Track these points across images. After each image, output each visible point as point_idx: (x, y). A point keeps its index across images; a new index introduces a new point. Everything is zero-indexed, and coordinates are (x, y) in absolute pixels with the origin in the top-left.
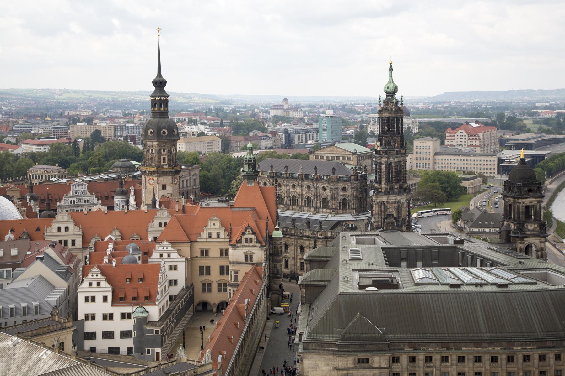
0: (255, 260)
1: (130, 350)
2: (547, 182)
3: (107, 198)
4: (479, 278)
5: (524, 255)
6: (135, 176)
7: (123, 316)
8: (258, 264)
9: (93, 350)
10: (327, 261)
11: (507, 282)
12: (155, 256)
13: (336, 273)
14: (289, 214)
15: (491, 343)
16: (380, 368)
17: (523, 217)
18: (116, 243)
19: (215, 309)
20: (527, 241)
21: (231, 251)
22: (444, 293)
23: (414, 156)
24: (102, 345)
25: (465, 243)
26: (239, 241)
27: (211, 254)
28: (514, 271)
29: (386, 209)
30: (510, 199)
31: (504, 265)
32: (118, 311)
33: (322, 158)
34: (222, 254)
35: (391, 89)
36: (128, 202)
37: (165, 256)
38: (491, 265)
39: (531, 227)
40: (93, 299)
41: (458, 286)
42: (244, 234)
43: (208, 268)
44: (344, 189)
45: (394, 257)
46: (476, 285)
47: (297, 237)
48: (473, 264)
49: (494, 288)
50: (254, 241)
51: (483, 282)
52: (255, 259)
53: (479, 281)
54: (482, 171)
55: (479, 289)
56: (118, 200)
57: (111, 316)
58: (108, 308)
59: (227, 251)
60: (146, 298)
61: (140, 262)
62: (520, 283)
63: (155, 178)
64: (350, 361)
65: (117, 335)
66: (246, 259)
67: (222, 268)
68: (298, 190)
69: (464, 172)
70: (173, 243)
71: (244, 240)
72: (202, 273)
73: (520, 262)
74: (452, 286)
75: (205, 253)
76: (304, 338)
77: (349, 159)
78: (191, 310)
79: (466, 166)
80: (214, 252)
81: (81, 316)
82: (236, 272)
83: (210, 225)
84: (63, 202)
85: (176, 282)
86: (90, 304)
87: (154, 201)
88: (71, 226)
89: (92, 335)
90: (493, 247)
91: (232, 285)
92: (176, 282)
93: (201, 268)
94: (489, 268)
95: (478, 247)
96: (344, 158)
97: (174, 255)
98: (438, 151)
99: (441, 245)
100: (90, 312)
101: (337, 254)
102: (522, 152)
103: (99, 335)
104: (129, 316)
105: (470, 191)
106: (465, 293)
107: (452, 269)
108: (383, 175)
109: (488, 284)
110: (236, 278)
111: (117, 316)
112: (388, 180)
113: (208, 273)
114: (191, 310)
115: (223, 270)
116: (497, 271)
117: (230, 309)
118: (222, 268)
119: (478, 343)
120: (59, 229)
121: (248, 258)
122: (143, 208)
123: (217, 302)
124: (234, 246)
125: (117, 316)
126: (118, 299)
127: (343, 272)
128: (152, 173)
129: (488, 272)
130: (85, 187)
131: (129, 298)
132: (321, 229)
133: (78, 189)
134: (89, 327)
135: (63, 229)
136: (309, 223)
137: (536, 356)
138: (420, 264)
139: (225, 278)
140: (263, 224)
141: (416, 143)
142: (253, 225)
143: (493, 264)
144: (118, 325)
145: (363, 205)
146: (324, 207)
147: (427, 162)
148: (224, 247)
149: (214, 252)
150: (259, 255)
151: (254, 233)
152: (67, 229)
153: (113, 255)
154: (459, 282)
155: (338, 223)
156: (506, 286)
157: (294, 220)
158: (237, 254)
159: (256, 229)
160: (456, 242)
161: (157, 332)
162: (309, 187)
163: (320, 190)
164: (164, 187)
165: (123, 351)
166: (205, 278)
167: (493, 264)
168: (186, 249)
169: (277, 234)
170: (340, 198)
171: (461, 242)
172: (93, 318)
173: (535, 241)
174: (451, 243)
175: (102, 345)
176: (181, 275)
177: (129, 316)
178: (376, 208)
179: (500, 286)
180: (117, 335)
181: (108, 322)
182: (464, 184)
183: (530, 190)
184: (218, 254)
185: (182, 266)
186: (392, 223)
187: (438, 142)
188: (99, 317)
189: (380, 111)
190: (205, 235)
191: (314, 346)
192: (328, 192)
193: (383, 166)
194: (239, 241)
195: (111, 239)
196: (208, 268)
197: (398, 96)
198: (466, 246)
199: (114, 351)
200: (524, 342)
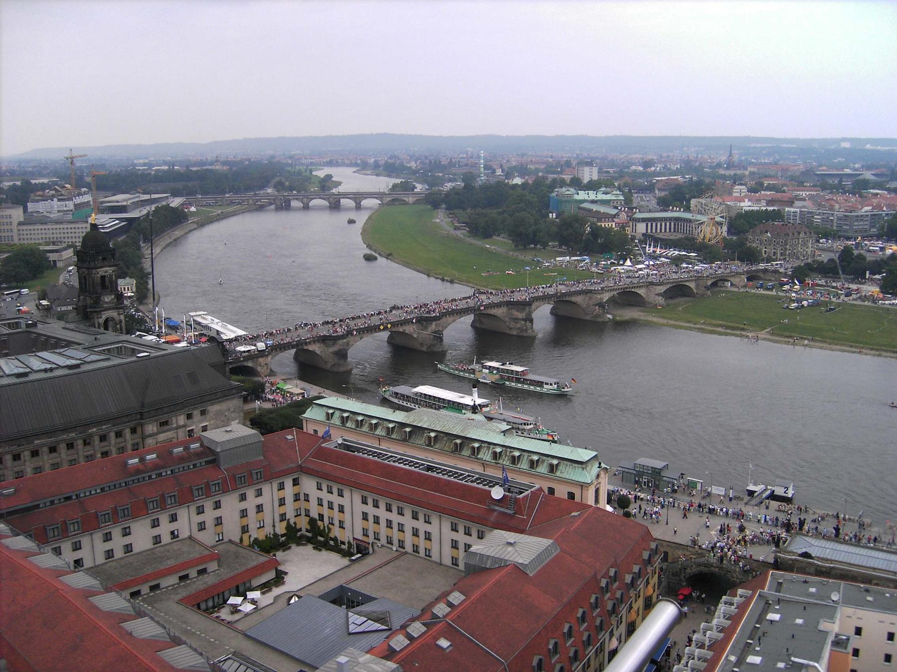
4: (50, 362)
5: (102, 330)
11: (79, 362)
20: (105, 315)
22: (9, 385)
25: (40, 326)
30: (84, 270)
31: (80, 344)
38: (66, 346)
39: (108, 298)
41: (25, 375)
46: (46, 370)
49: (67, 372)
51: (54, 366)
53: (48, 366)
54: (74, 240)
55: (49, 375)
62: (94, 361)
69: (54, 243)
73: (96, 339)
74: (19, 375)
79: (55, 236)
90: (71, 326)
94: (62, 350)
95: (54, 328)
98: (22, 220)
99: (11, 331)
105: (60, 265)
106: (33, 381)
109: (60, 367)
116: (70, 352)
129: (60, 354)
137: (112, 435)
143: (69, 344)
147: (10, 234)
154: (28, 370)
160: (28, 326)
167: (69, 344)
171: (34, 325)
179: (70, 367)
182: (52, 257)
183: (104, 259)
187: (20, 211)
198: (41, 329)
200: (98, 423)
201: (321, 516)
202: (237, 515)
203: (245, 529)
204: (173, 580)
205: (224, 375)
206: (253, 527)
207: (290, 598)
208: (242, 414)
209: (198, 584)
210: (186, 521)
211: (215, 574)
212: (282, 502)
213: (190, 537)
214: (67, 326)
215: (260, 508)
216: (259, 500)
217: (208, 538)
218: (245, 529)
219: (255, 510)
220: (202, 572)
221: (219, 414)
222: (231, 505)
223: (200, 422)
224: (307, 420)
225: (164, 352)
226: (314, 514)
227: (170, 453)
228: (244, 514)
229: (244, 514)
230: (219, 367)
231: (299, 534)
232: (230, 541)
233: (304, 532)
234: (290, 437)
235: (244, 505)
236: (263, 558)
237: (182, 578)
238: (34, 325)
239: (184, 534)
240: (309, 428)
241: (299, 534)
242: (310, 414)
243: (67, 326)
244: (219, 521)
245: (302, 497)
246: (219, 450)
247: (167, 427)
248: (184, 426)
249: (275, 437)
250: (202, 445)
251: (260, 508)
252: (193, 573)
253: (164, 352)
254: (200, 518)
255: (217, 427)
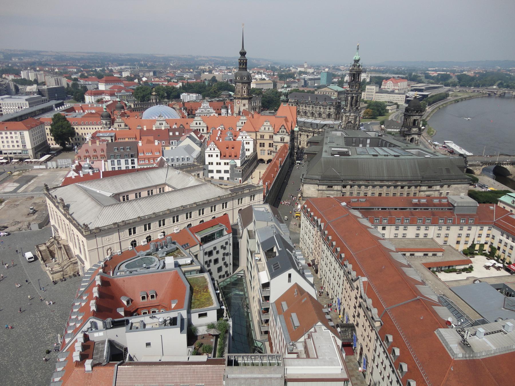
0: (285, 141)
1: (228, 178)
2: (427, 108)
3: (218, 109)
6: (231, 99)
7: (225, 164)
8: (287, 143)
9: (212, 177)
10: (318, 143)
12: (239, 138)
13: (322, 148)
14: (303, 120)
15: (388, 181)
16: (337, 191)
17: (411, 125)
18: (221, 131)
19: (266, 162)
21: (274, 136)
23: (366, 93)
24: (216, 176)
26: (278, 132)
27: (265, 138)
28: (404, 149)
29: (349, 119)
32: (223, 162)
33: (321, 93)
34: (270, 138)
35: (357, 58)
36: (228, 112)
37: (244, 137)
38: (393, 147)
40: (212, 156)
41: (377, 155)
42: (280, 129)
43: (264, 144)
44: (330, 109)
45: (349, 142)
46: (385, 155)
47: (306, 131)
48: (386, 146)
49: (393, 157)
50: (285, 132)
52: (285, 141)
53: (386, 154)
55: (386, 157)
56: (223, 111)
57: (220, 164)
58: (218, 160)
59: (272, 136)
60: (235, 156)
61: (232, 140)
63: (240, 101)
64: (324, 187)
65: (223, 172)
66: (281, 140)
67: (270, 144)
68: (308, 108)
70: (248, 132)
71: (280, 132)
72: (260, 146)
74: (374, 155)
75: (262, 137)
76: (304, 176)
77: (334, 94)
78: (255, 163)
80: (267, 137)
81: (207, 163)
82: (276, 146)
83: (265, 124)
84: (198, 111)
85: (249, 150)
86: (210, 158)
87: (239, 112)
88: (202, 122)
89: (212, 171)
91: (273, 152)
92: (249, 150)
93: (261, 144)
95: (390, 139)
96: (331, 93)
97: (248, 137)
100: (211, 161)
101: (323, 140)
102: (417, 93)
103: (215, 172)
104: (228, 164)
107: (375, 148)
108: (349, 102)
109: (391, 155)
110: (276, 149)
111: (222, 164)
112: (351, 105)
113: (264, 146)
114: (255, 163)
115: (270, 145)
117: (273, 163)
118: (270, 144)
119: (382, 181)
120: (196, 124)
121: (282, 139)
122: (235, 115)
123: (267, 159)
124: (276, 134)
125: (222, 164)
126: (223, 156)
127: (325, 148)
128: (239, 98)
129: (391, 150)
130: (208, 104)
131: (227, 156)
132: (317, 127)
133: (205, 105)
134: (210, 168)
135: (198, 124)
136: (311, 124)
138: (361, 145)
139: (272, 149)
140: (289, 124)
141: (367, 87)
142: (285, 125)
143: (395, 146)
144: (223, 168)
145: (338, 116)
146: (320, 117)
148: (272, 134)
149: (267, 137)
150: (287, 139)
151: (285, 129)
152: (200, 124)
153: (220, 137)
155: (325, 125)
156: (398, 156)
157: (305, 123)
158: (277, 138)
159: (286, 127)
160: (379, 136)
161: (240, 171)
162: (313, 107)
163: (318, 109)
164: (244, 105)
165: (225, 179)
166: (262, 148)
167: (395, 146)
168: (254, 135)
169: (296, 129)
170: (327, 113)
172: (212, 164)
173: (416, 137)
174: (377, 135)
175: (216, 176)
176: (251, 147)
177: (228, 164)
178: (344, 118)
180: (223, 172)
181: (219, 166)
184: (268, 138)
185: (252, 143)
186: (351, 126)
188: (215, 164)
189: (351, 71)
190: (262, 128)
191: (310, 181)
192: (322, 110)
193: (349, 98)
194: (278, 132)
195: (219, 129)
196: (264, 144)
197: (360, 63)
199: (221, 178)
201: (499, 248)
202: (457, 235)
203: (458, 242)
204: (421, 254)
205: (463, 171)
206: (462, 242)
207: (475, 280)
208: (467, 191)
209: (431, 259)
210: (432, 231)
211: (440, 257)
212: (480, 236)
213: (432, 239)
214: (396, 138)
215: (468, 236)
216: (469, 232)
217: (440, 241)
218: (458, 242)
219: (466, 235)
220: (434, 255)
221: (455, 188)
222: (454, 230)
223: (447, 190)
224: (501, 202)
225: (437, 157)
226: (495, 245)
227: (432, 201)
228: (460, 236)
229: (460, 236)
230: (461, 168)
231: (483, 252)
232: (450, 245)
233: (487, 252)
234: (492, 207)
235: (460, 232)
236: (464, 258)
237: (425, 255)
238: (381, 136)
239: (430, 236)
240: (501, 205)
241: (483, 252)
242: (503, 198)
243: (396, 138)
244: (447, 236)
245: (491, 236)
246: (455, 205)
247: (430, 189)
248: (439, 190)
249: (484, 205)
250: (448, 201)
251: (468, 236)
252: (430, 254)
253: (437, 157)
254: (439, 232)
255: (454, 195)
